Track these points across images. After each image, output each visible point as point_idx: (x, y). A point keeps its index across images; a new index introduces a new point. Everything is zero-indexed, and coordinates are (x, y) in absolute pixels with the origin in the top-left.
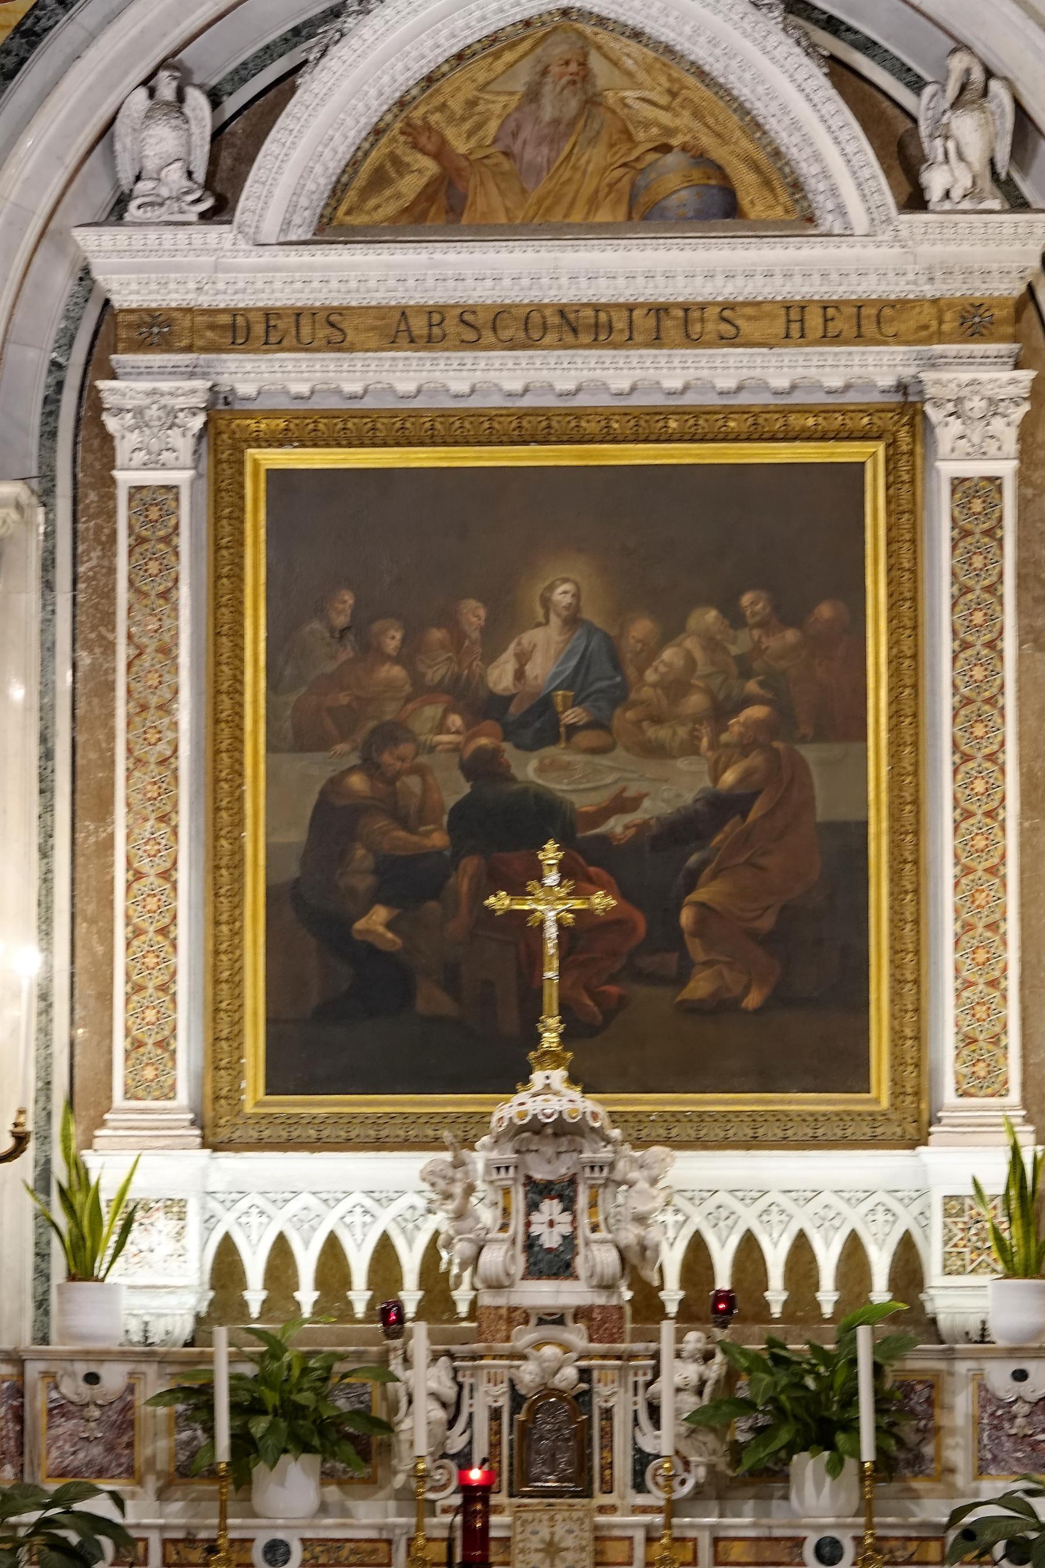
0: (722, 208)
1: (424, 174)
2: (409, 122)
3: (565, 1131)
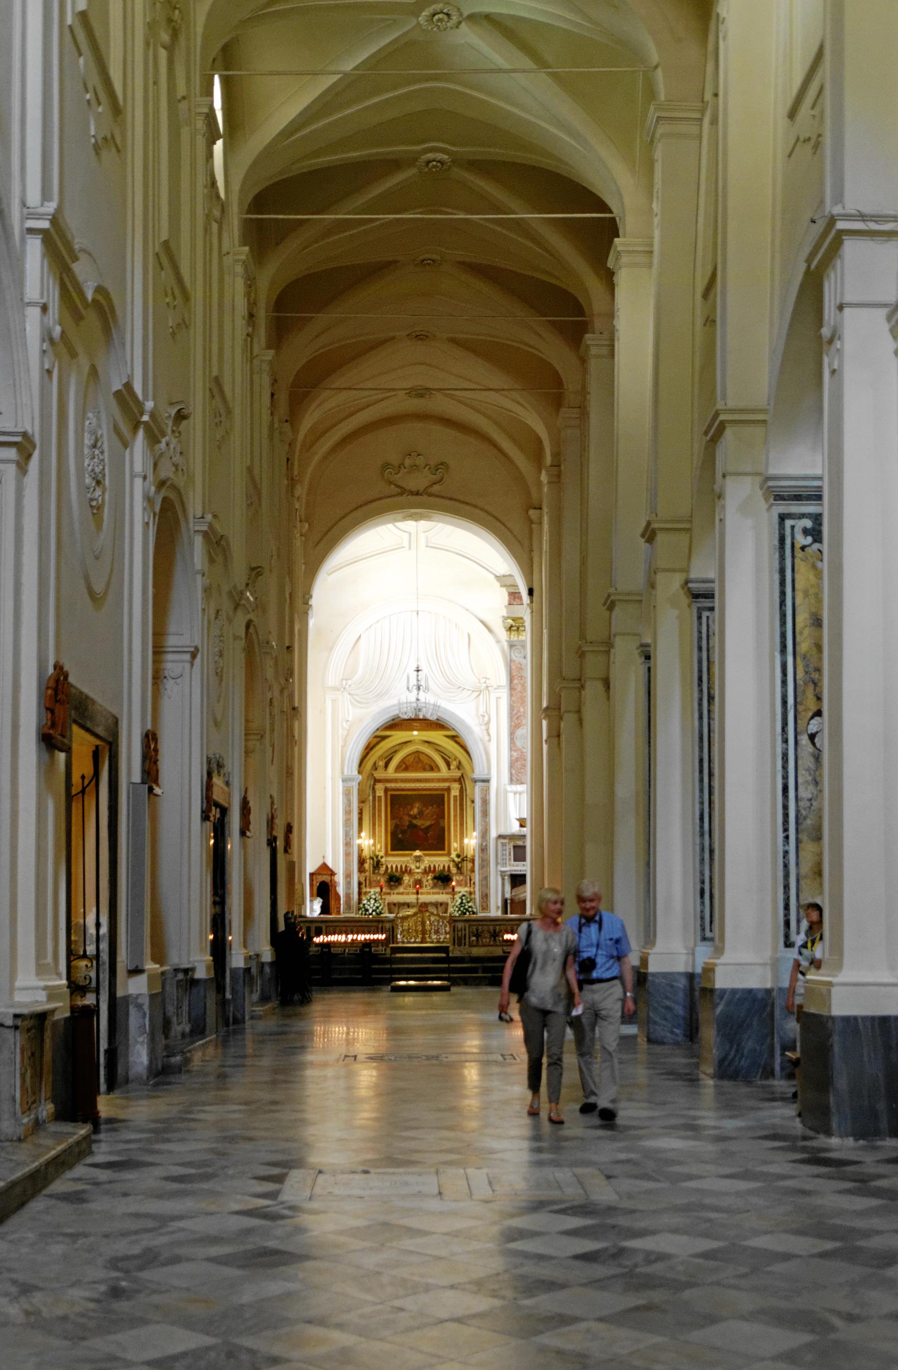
0: (432, 769)
1: (404, 766)
2: (403, 761)
3: (420, 856)
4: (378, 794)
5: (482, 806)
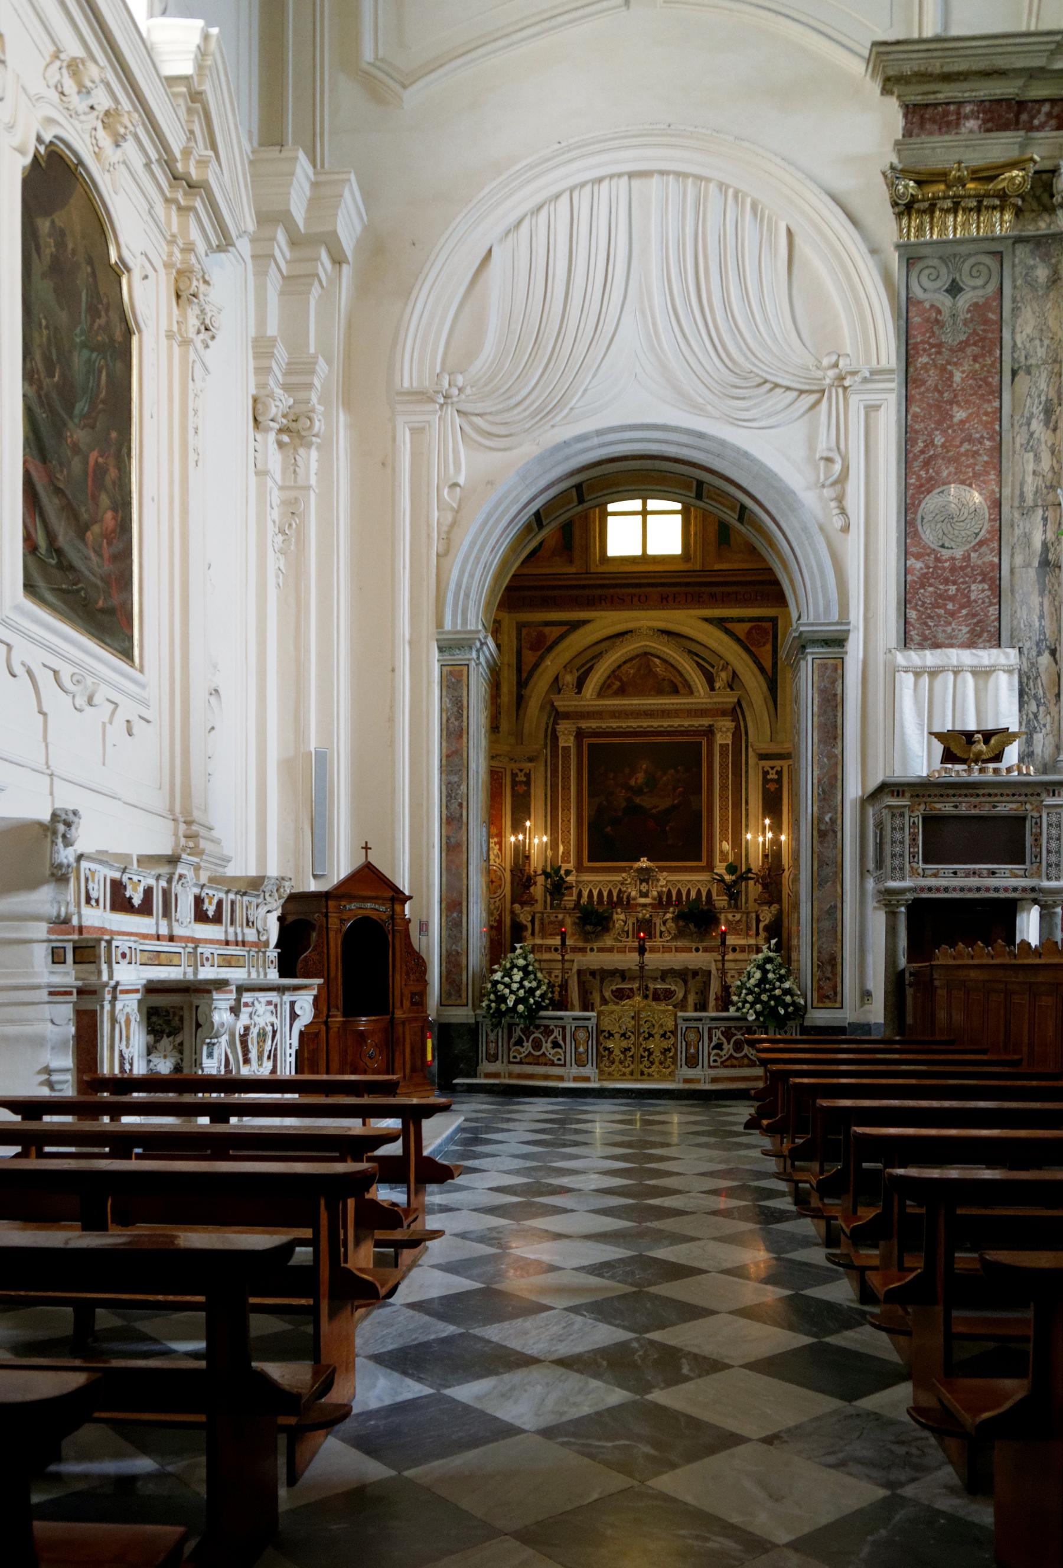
0: (675, 691)
1: (618, 684)
2: (614, 674)
3: (647, 870)
4: (562, 744)
5: (823, 712)
